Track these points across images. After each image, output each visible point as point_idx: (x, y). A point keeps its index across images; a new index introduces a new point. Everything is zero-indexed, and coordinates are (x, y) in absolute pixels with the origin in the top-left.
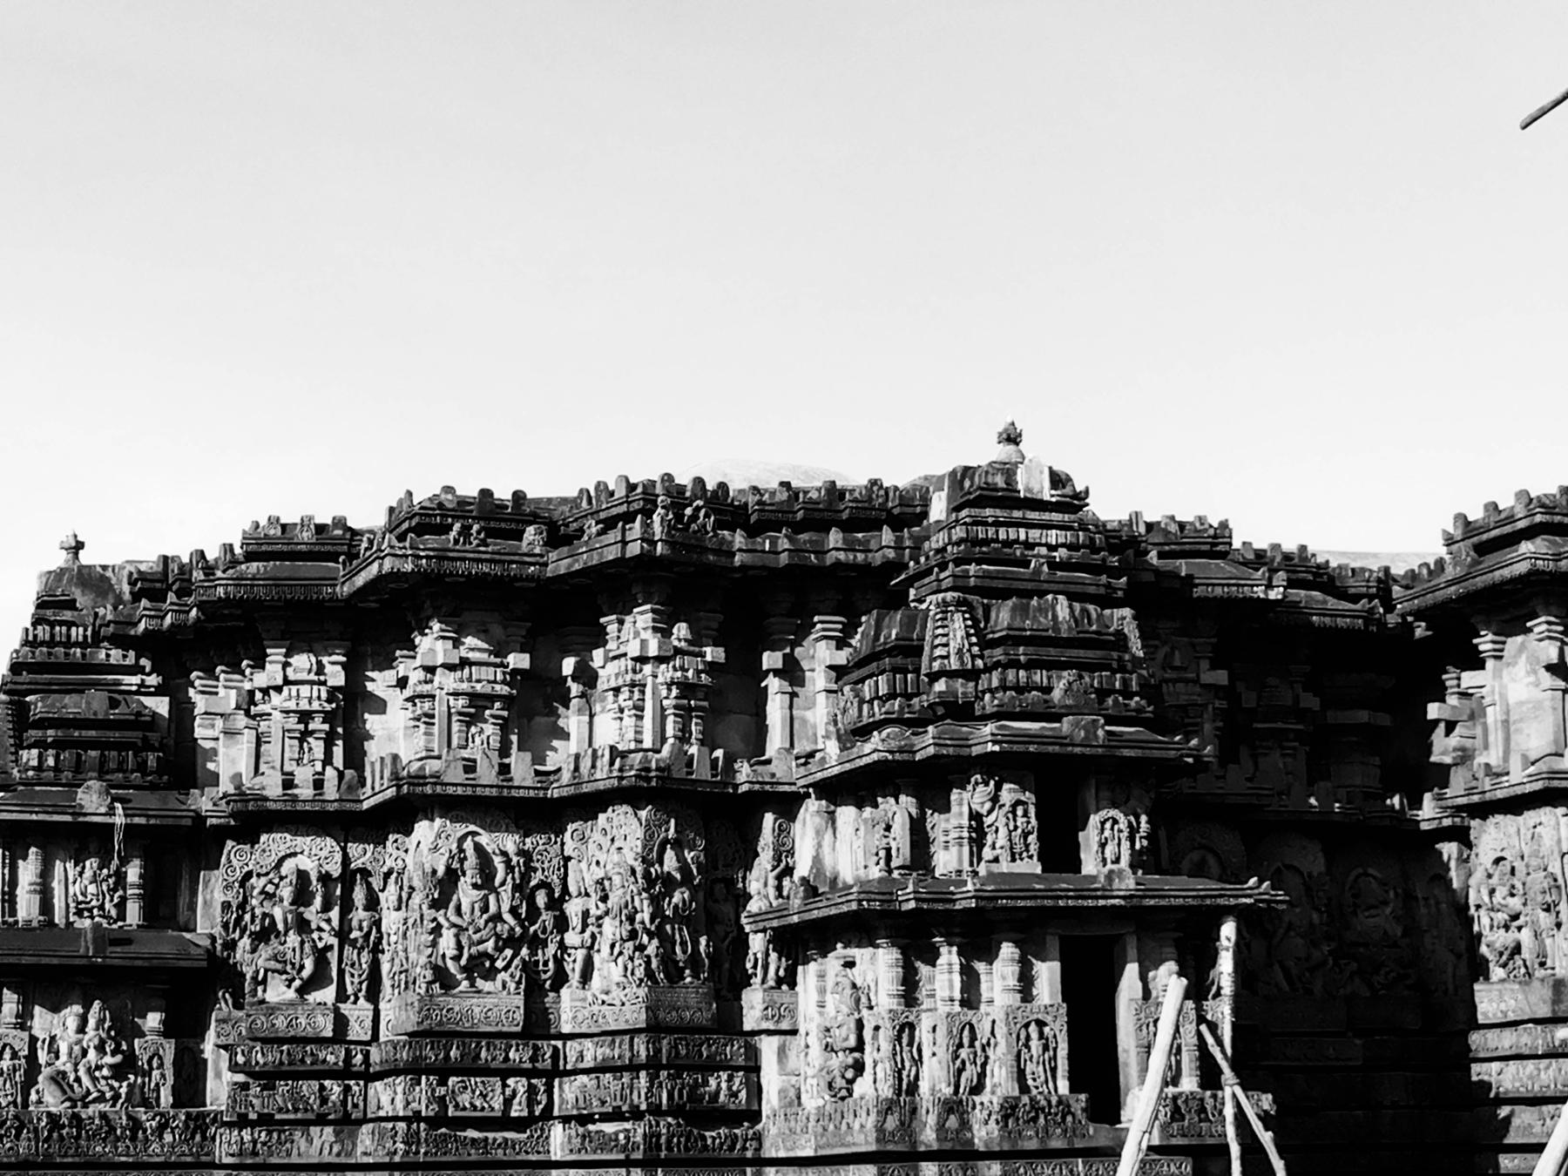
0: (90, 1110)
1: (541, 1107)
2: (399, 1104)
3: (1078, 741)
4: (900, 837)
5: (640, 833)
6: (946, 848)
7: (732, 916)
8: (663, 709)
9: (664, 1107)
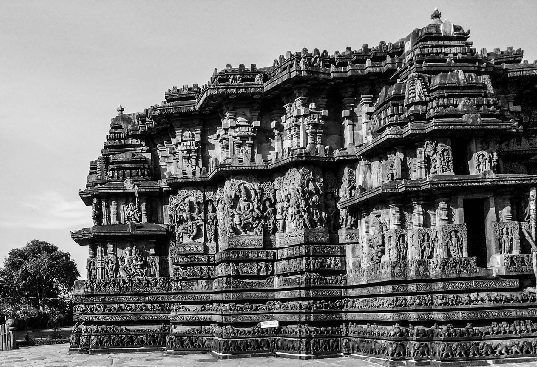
0: (135, 278)
1: (270, 271)
2: (224, 272)
3: (469, 123)
4: (397, 170)
5: (300, 177)
6: (415, 171)
7: (334, 205)
8: (307, 134)
9: (312, 270)
